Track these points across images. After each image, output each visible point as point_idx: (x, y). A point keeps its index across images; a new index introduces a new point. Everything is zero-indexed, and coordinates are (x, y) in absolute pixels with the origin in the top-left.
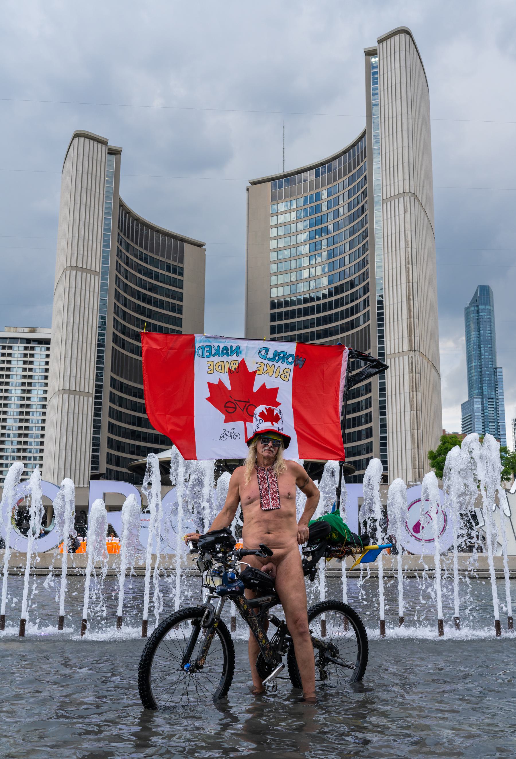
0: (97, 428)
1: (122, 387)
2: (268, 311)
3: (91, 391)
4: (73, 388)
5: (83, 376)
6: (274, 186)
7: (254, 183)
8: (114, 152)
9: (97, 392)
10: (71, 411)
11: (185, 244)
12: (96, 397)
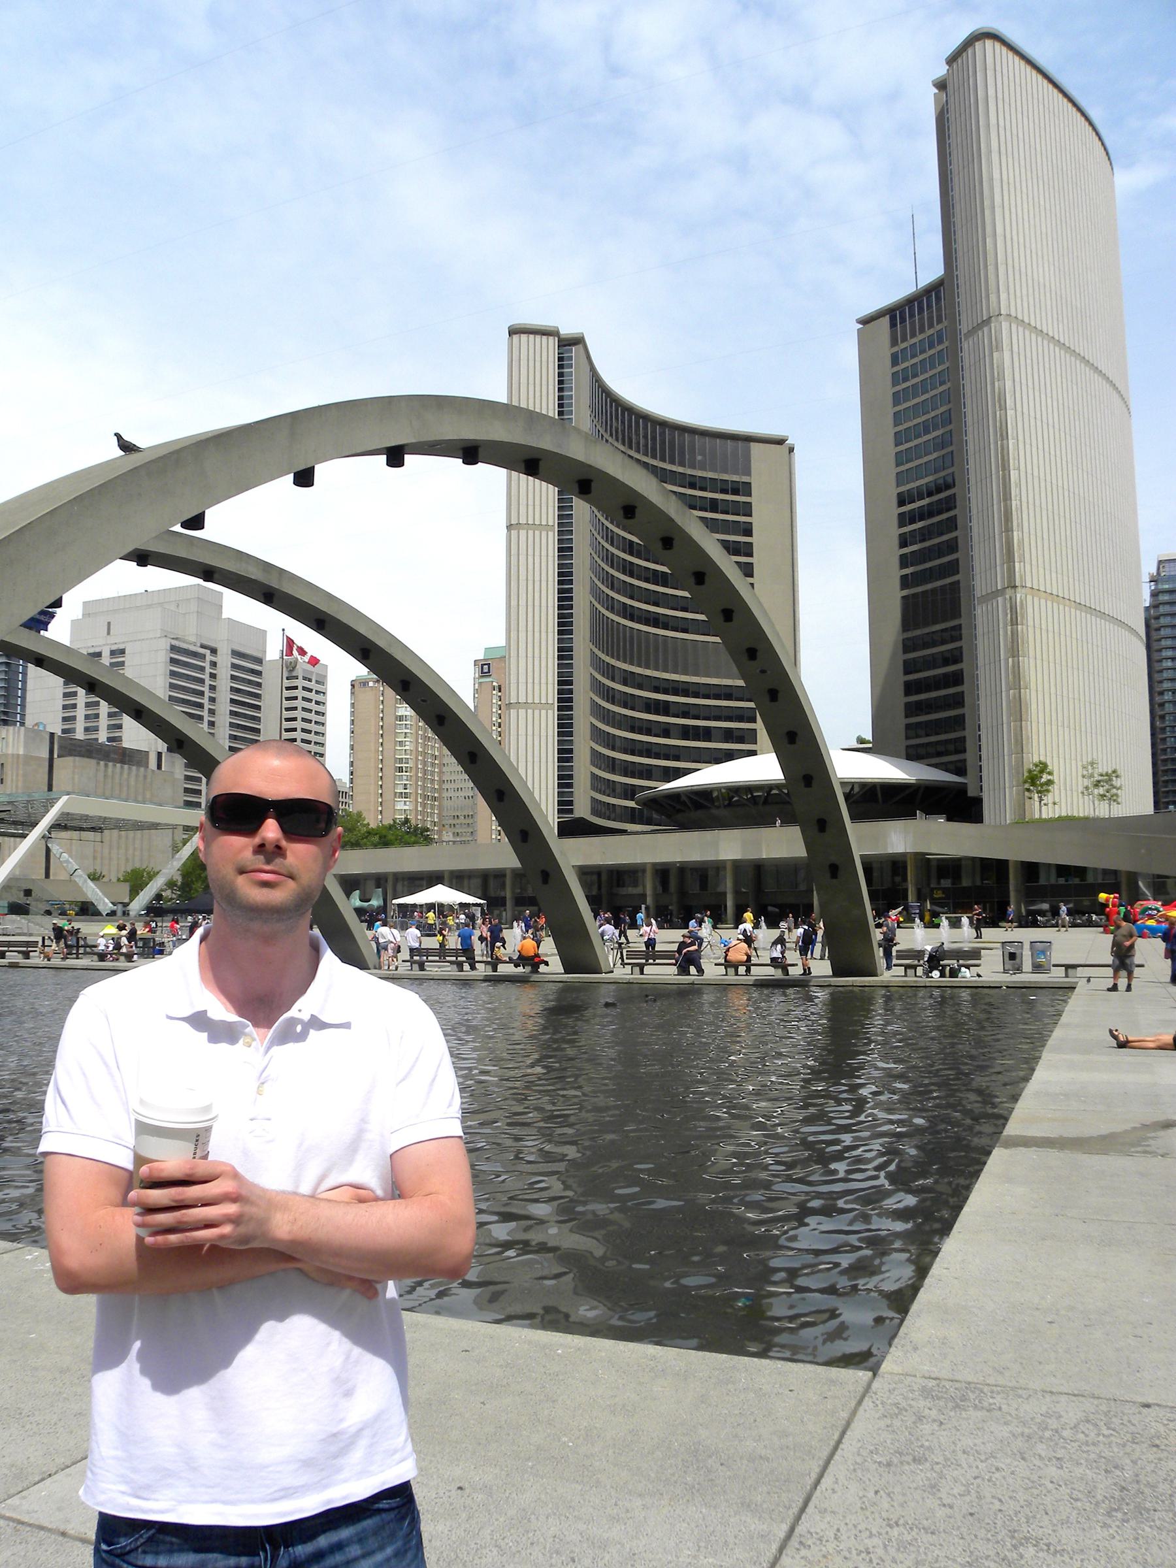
4: (522, 700)
5: (536, 681)
6: (893, 325)
7: (865, 321)
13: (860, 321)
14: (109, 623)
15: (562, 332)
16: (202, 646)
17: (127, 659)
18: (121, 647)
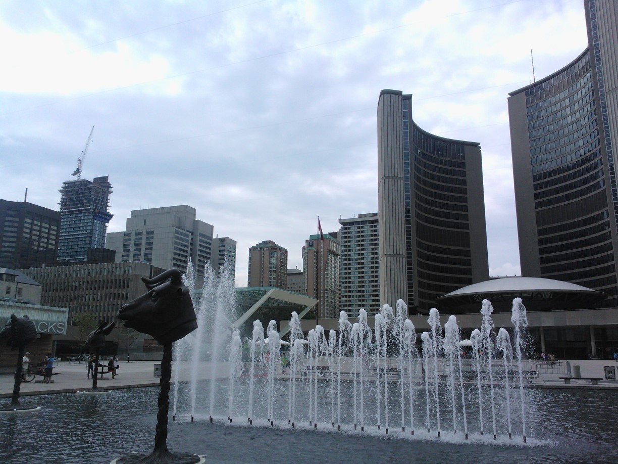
0: (410, 278)
1: (428, 248)
2: (531, 184)
3: (404, 254)
4: (392, 253)
6: (527, 95)
7: (512, 94)
8: (409, 98)
9: (408, 253)
10: (392, 267)
11: (465, 146)
12: (408, 257)
13: (510, 94)
14: (145, 220)
15: (403, 94)
16: (187, 231)
17: (155, 235)
18: (152, 230)
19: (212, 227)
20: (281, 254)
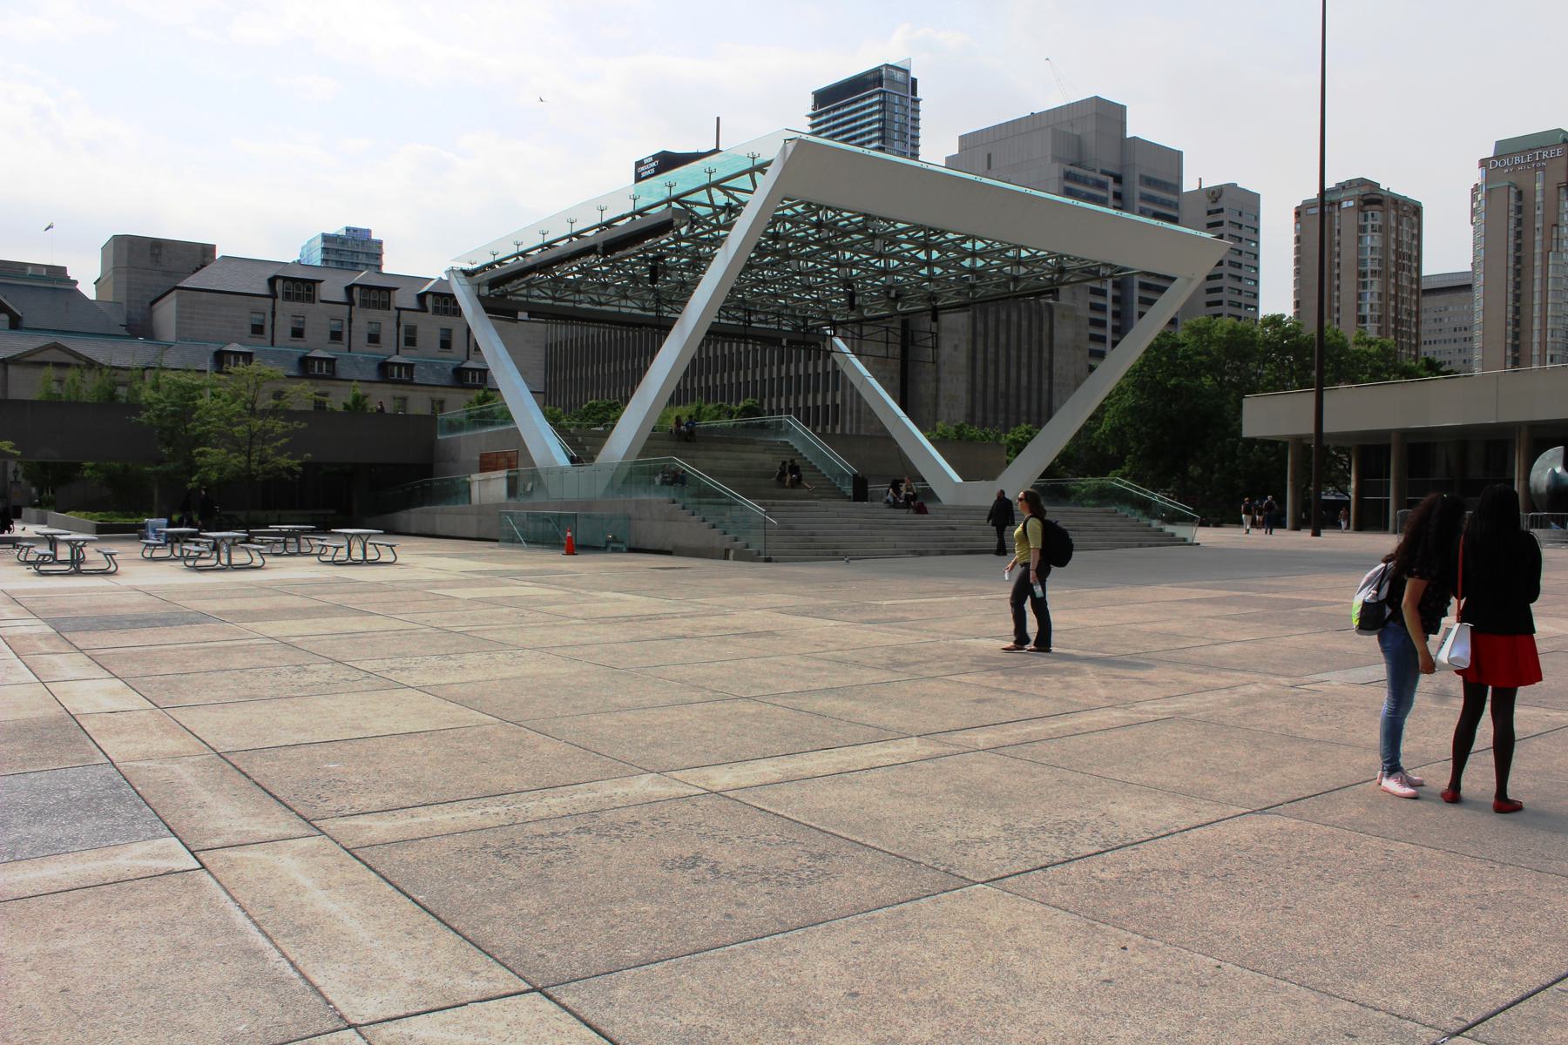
14: (989, 156)
19: (1179, 154)
20: (1399, 223)
